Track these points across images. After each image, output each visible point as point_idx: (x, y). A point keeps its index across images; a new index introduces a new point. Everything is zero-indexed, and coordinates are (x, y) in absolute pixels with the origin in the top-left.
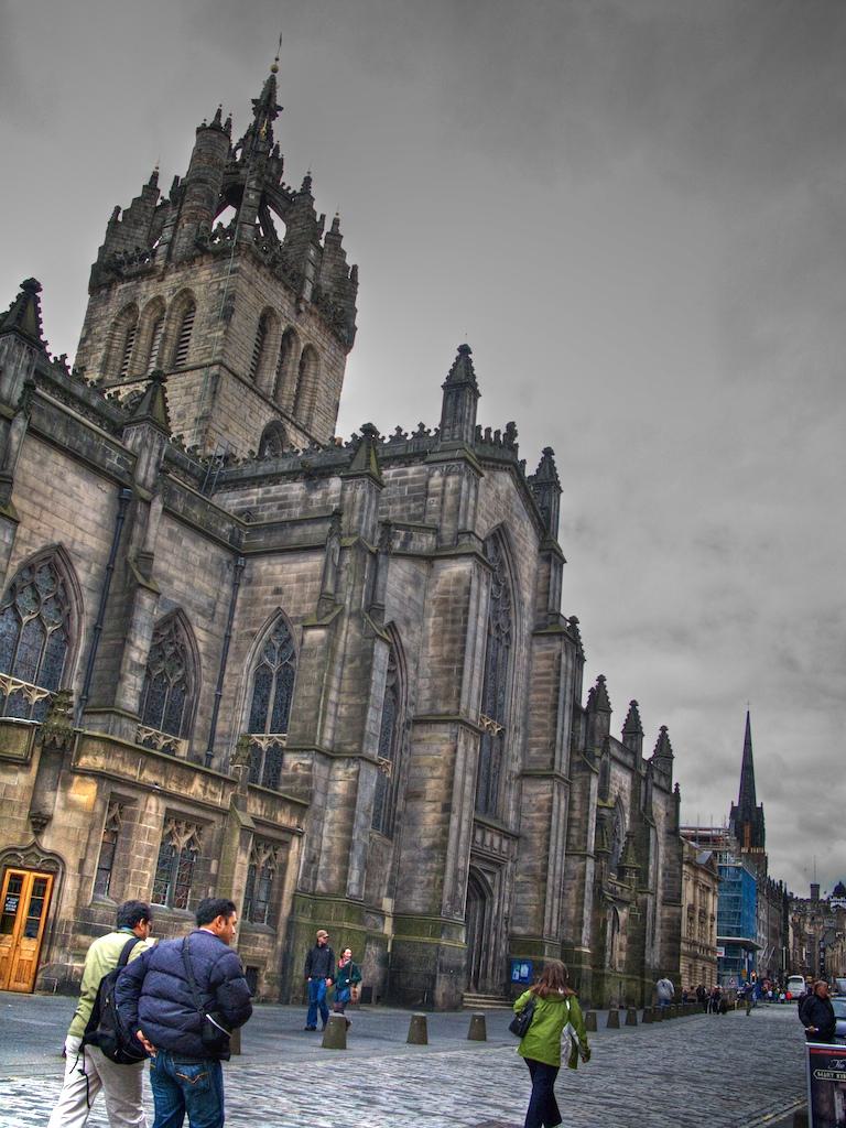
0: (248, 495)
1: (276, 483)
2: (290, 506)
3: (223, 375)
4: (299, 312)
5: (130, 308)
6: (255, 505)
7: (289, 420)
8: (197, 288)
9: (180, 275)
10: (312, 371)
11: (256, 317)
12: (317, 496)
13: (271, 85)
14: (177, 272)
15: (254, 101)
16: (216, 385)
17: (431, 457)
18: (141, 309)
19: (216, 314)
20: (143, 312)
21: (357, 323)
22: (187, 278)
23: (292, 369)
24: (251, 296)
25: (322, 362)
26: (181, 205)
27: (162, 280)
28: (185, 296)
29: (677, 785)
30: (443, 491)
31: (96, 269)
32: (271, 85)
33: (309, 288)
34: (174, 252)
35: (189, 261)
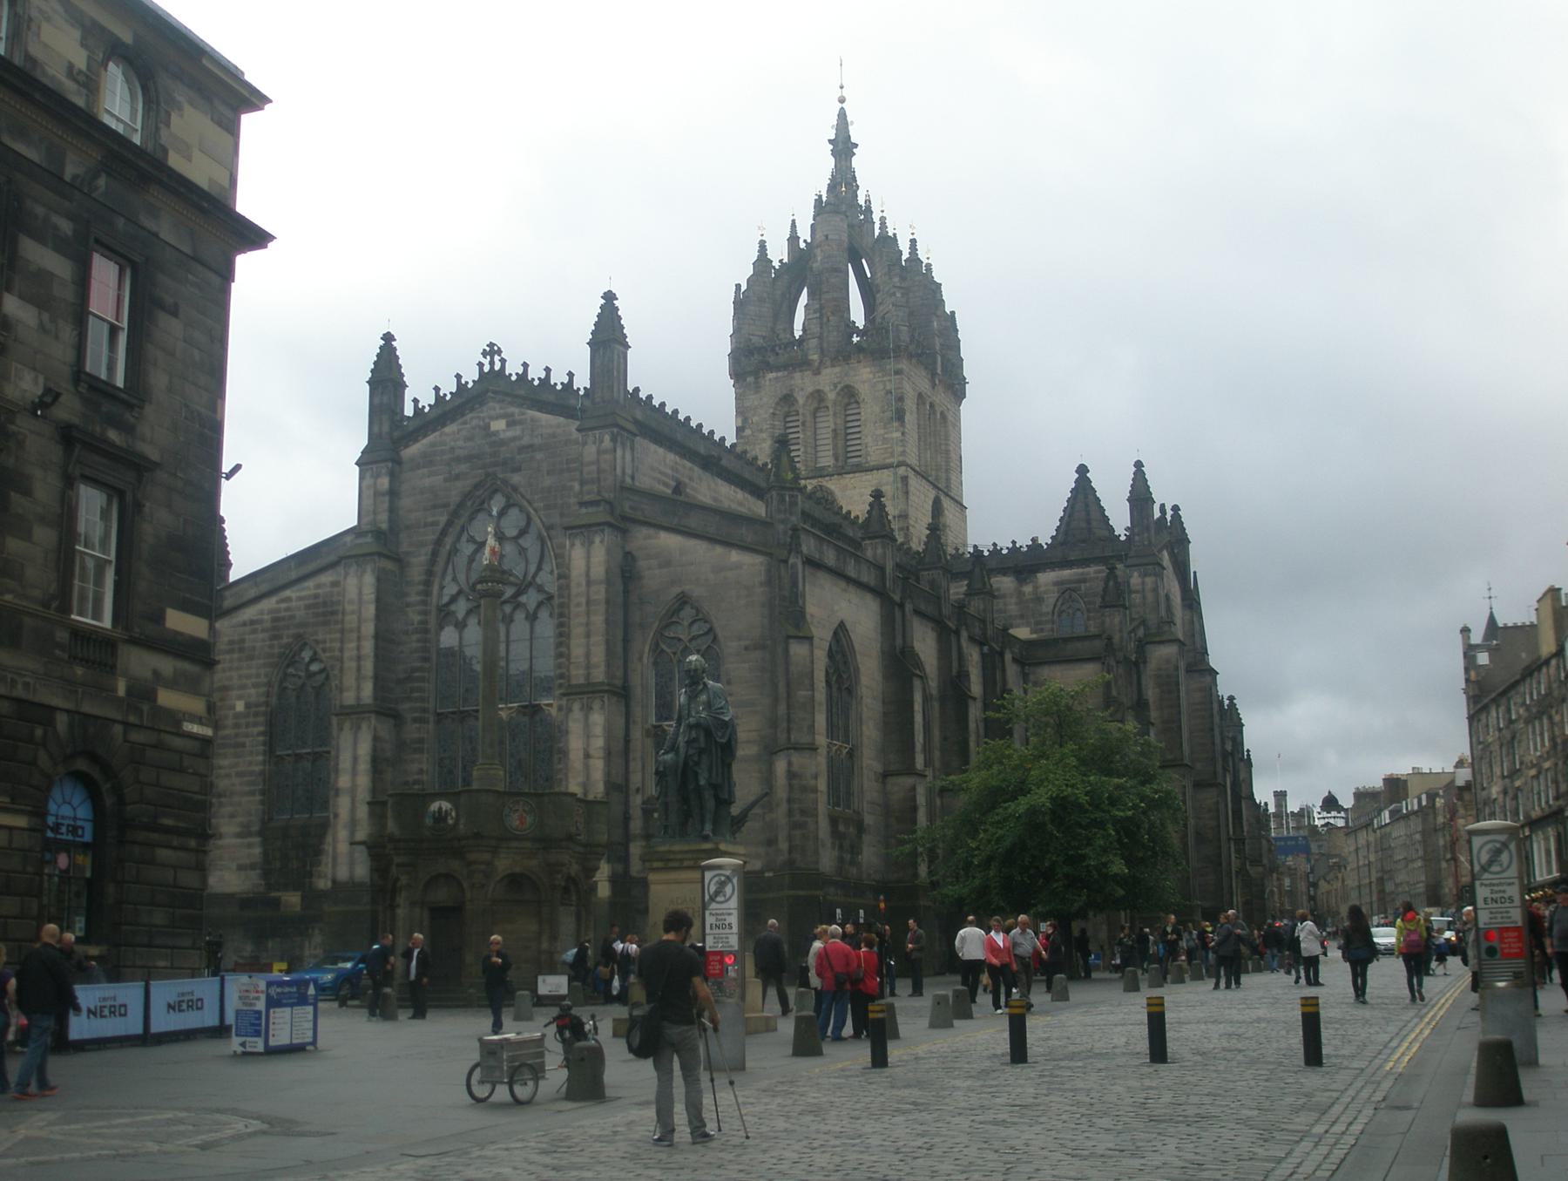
4: (934, 386)
5: (788, 399)
9: (837, 369)
12: (1028, 589)
14: (833, 366)
16: (907, 485)
17: (1129, 562)
18: (801, 401)
19: (888, 414)
20: (804, 405)
22: (846, 375)
28: (846, 390)
29: (1248, 751)
30: (1143, 590)
32: (843, 120)
34: (825, 345)
35: (847, 359)
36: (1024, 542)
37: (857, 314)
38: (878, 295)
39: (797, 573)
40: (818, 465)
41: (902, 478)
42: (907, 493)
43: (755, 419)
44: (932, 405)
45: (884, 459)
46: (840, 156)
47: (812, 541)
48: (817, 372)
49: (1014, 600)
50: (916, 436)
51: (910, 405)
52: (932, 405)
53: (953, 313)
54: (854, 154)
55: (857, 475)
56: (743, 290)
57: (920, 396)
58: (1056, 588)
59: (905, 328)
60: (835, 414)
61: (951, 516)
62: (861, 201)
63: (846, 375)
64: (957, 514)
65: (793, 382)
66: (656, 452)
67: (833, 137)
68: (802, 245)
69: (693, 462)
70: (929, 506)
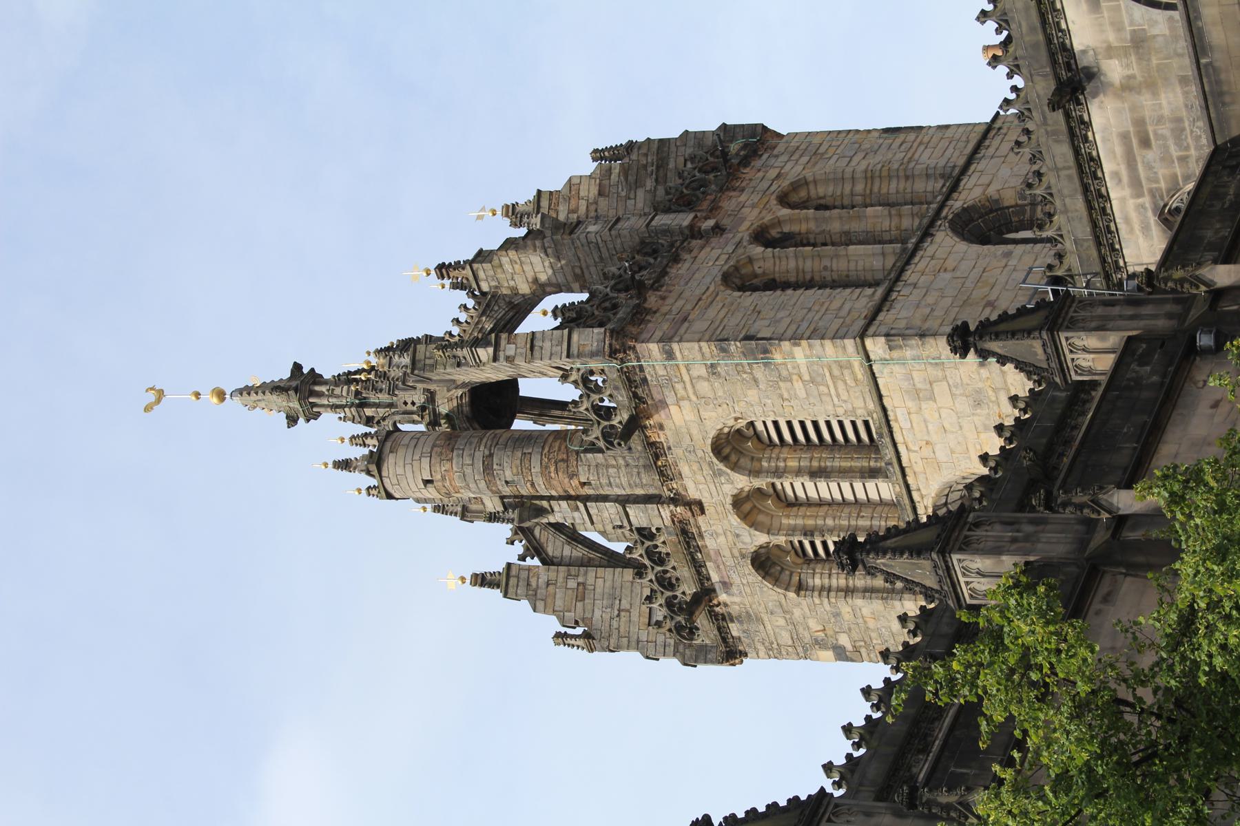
0: (1127, 220)
1: (1097, 161)
2: (1140, 123)
4: (718, 229)
5: (764, 562)
6: (1146, 200)
7: (942, 206)
8: (707, 423)
9: (685, 469)
10: (830, 189)
11: (749, 299)
12: (1114, 70)
15: (292, 420)
18: (762, 539)
19: (759, 372)
21: (712, 126)
23: (835, 223)
24: (711, 313)
25: (809, 175)
26: (542, 498)
27: (700, 504)
28: (726, 451)
31: (693, 657)
34: (639, 492)
35: (656, 451)
41: (891, 348)
43: (814, 625)
44: (762, 237)
45: (856, 380)
46: (313, 405)
49: (1146, 100)
52: (762, 237)
53: (598, 155)
56: (563, 630)
59: (575, 337)
60: (778, 473)
61: (1005, 172)
65: (727, 553)
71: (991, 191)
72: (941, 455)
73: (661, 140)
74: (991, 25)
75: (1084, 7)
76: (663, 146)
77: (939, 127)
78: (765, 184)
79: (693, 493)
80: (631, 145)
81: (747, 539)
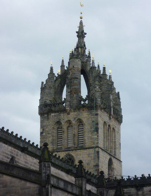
3: (100, 151)
4: (110, 119)
7: (112, 156)
9: (76, 113)
12: (140, 193)
13: (81, 23)
14: (74, 112)
15: (77, 32)
19: (93, 129)
22: (79, 115)
25: (116, 132)
27: (69, 114)
31: (40, 107)
32: (81, 23)
33: (112, 109)
34: (72, 105)
35: (79, 109)
36: (139, 176)
37: (84, 93)
38: (91, 87)
39: (48, 191)
40: (68, 146)
41: (97, 152)
42: (98, 157)
43: (47, 129)
44: (109, 126)
47: (55, 179)
48: (69, 114)
50: (103, 137)
51: (101, 126)
52: (109, 126)
53: (118, 93)
54: (85, 37)
55: (81, 150)
57: (105, 122)
58: (150, 193)
59: (100, 99)
62: (87, 53)
63: (79, 115)
64: (118, 164)
66: (4, 147)
67: (78, 31)
68: (66, 68)
69: (18, 150)
70: (107, 162)
71: (114, 164)
72: (78, 157)
73: (120, 105)
74: (148, 176)
75: (150, 190)
76: (120, 105)
77: (120, 152)
78: (115, 125)
79: (72, 114)
80: (119, 99)
81: (63, 121)
